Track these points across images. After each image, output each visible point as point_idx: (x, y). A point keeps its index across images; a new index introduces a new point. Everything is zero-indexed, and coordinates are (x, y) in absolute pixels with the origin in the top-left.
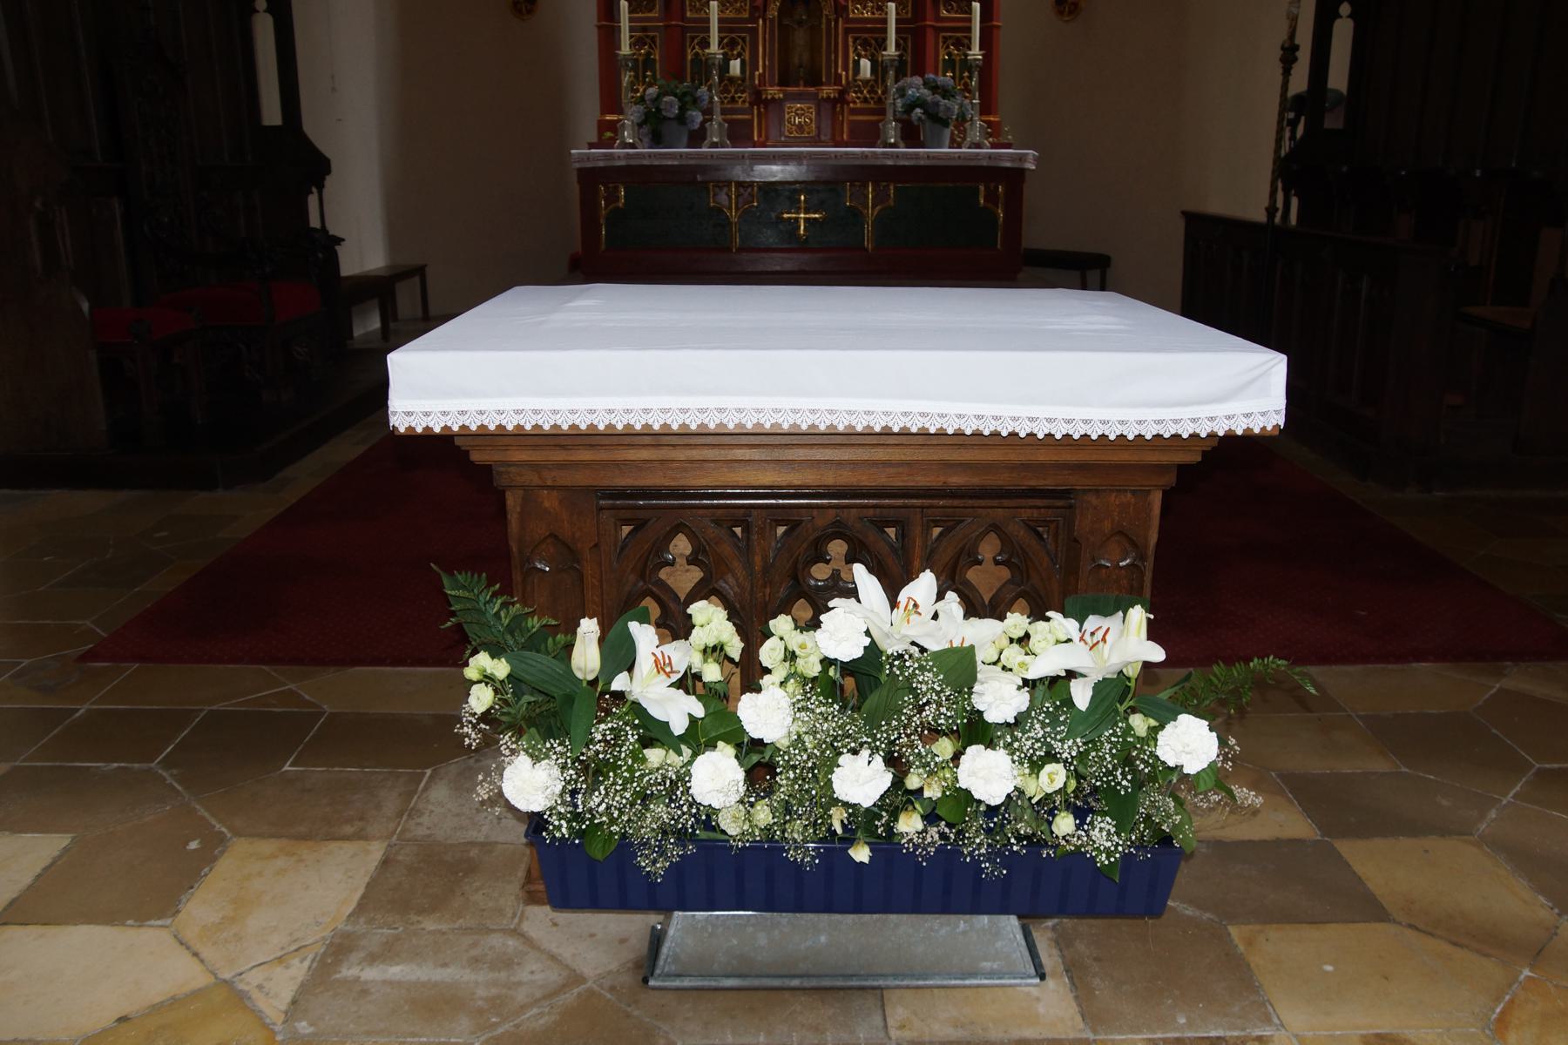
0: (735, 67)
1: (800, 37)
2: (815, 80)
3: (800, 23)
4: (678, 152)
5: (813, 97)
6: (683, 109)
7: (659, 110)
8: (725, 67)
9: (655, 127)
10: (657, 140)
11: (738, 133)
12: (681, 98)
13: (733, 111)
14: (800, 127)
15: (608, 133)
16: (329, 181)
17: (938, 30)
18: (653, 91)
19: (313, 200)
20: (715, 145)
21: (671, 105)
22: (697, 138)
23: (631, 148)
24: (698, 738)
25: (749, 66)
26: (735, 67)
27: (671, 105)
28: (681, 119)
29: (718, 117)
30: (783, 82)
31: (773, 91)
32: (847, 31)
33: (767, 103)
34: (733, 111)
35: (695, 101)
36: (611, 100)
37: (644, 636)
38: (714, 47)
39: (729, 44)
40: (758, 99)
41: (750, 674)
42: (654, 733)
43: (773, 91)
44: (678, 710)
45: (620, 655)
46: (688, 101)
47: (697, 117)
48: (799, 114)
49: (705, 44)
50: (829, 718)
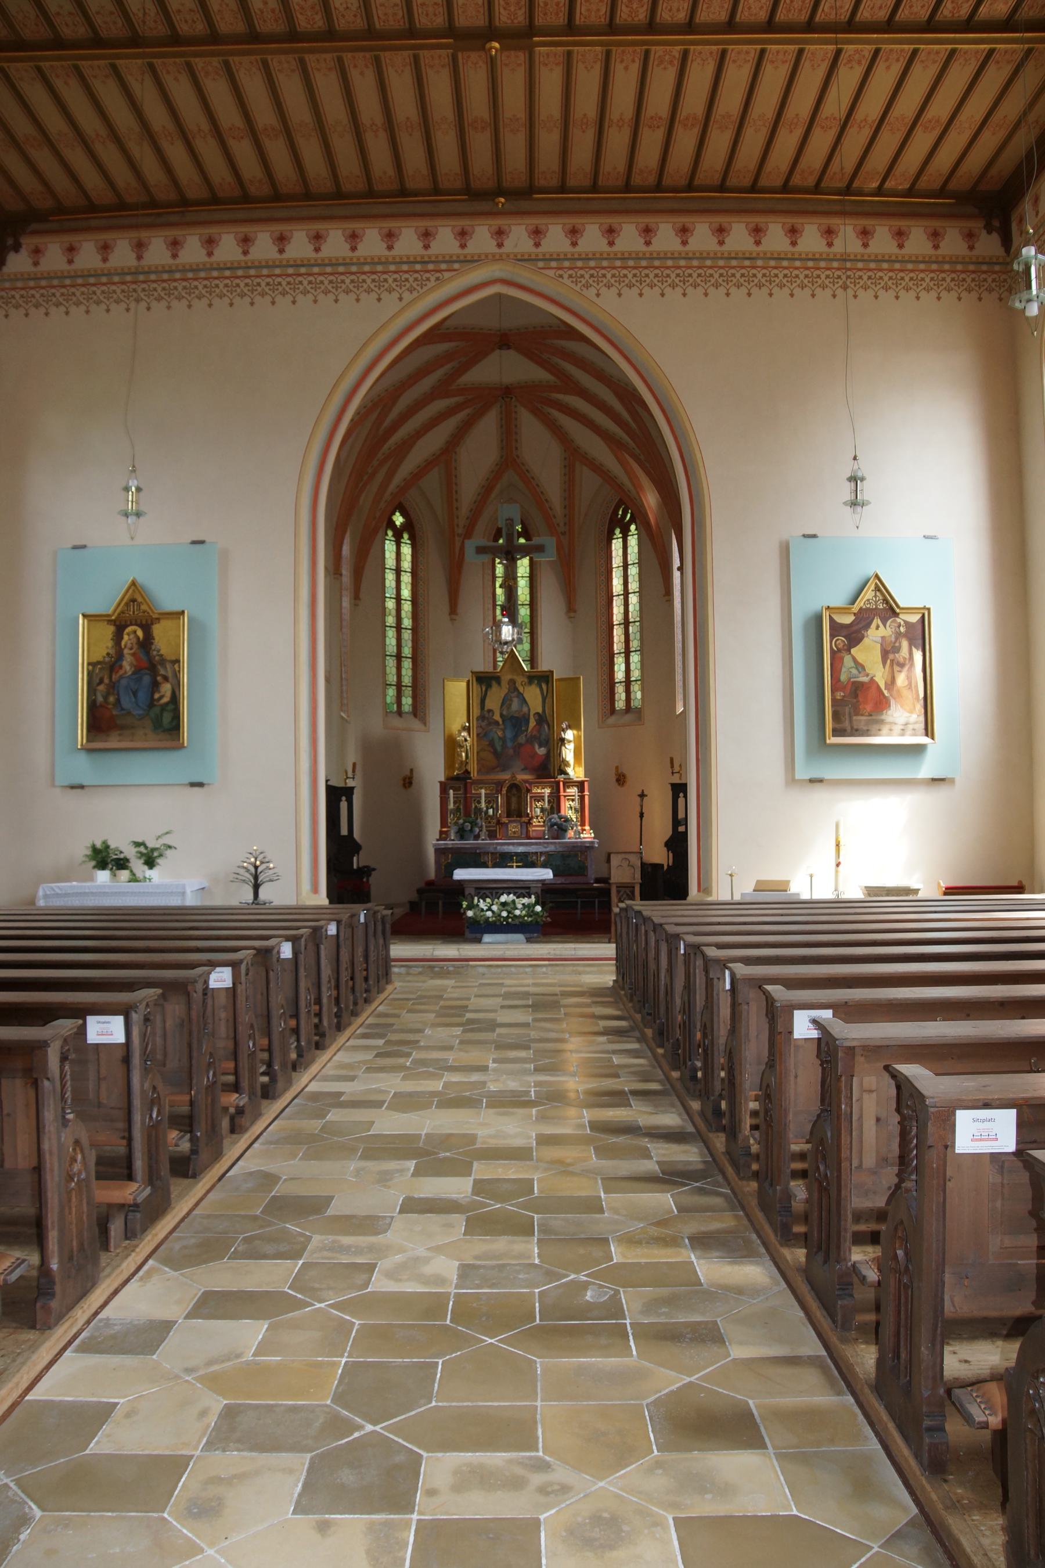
0: (491, 811)
1: (514, 800)
2: (520, 815)
3: (514, 795)
4: (471, 842)
5: (519, 821)
6: (472, 827)
7: (463, 828)
8: (486, 812)
9: (462, 834)
10: (462, 838)
11: (492, 835)
12: (471, 823)
13: (490, 827)
14: (514, 832)
15: (443, 836)
16: (361, 853)
17: (565, 796)
18: (461, 821)
19: (355, 859)
20: (483, 840)
21: (468, 826)
22: (477, 837)
23: (453, 842)
24: (487, 910)
25: (496, 810)
26: (491, 811)
27: (468, 826)
28: (471, 831)
29: (484, 829)
30: (508, 816)
31: (505, 820)
32: (531, 797)
33: (502, 824)
34: (490, 827)
35: (476, 824)
36: (444, 823)
37: (481, 901)
38: (483, 805)
39: (488, 802)
40: (499, 822)
41: (493, 904)
42: (482, 910)
43: (505, 820)
44: (485, 908)
45: (479, 901)
46: (474, 824)
47: (477, 830)
48: (514, 828)
49: (479, 802)
50: (501, 907)
